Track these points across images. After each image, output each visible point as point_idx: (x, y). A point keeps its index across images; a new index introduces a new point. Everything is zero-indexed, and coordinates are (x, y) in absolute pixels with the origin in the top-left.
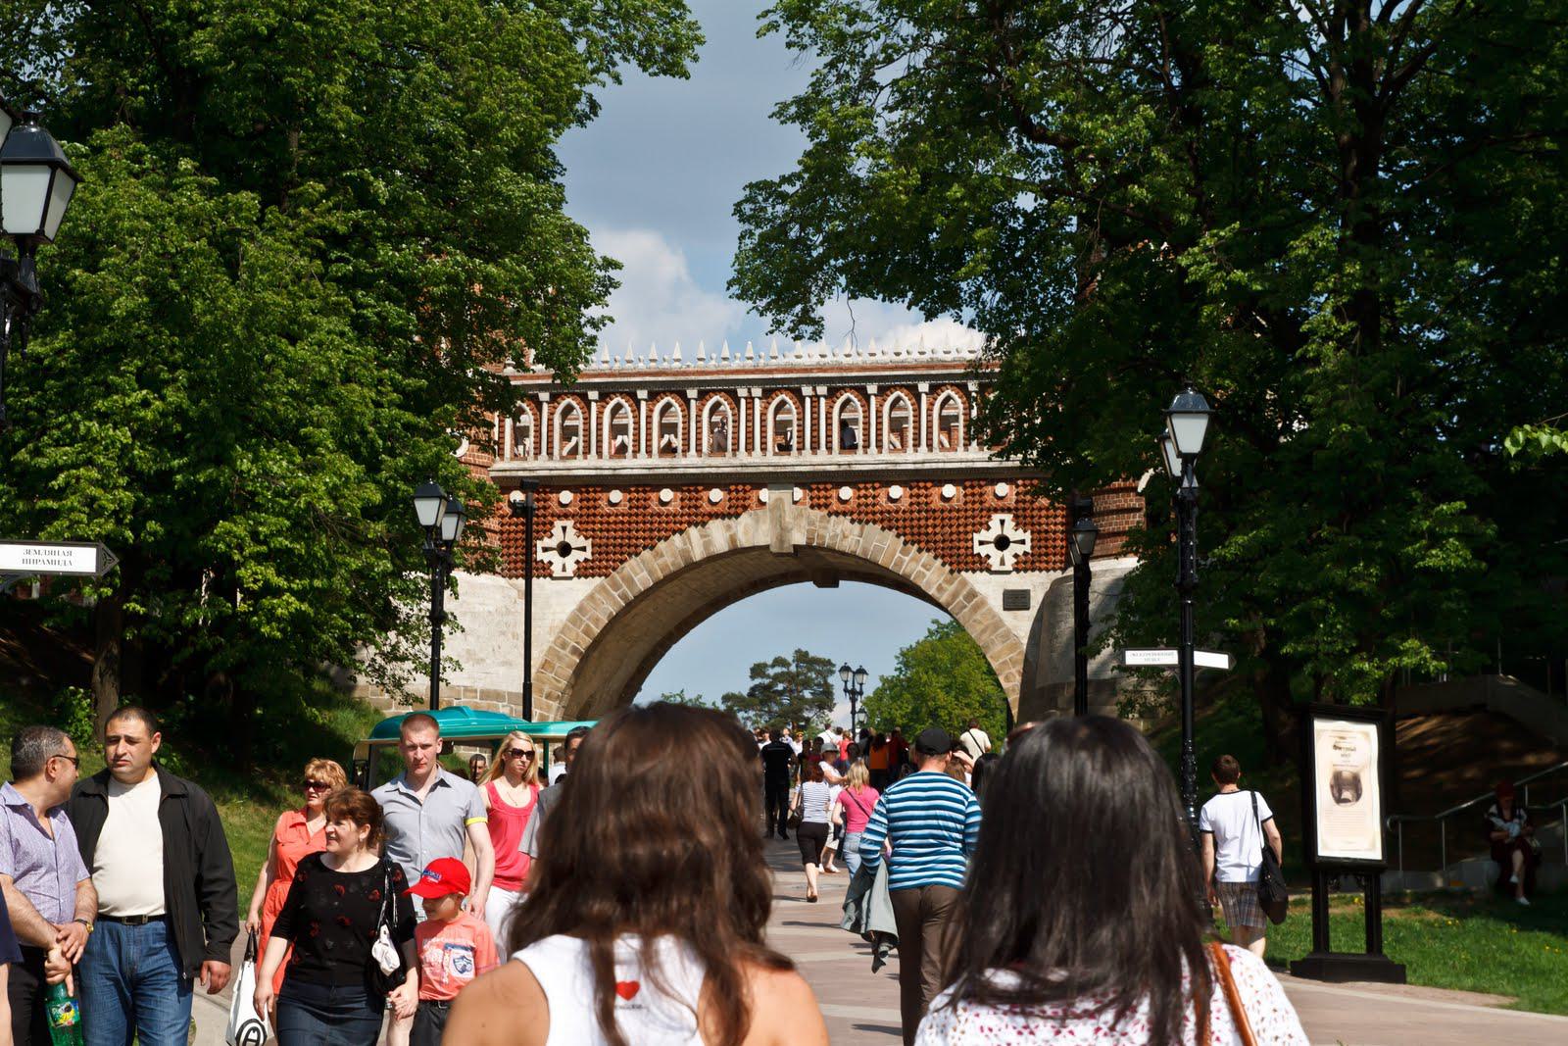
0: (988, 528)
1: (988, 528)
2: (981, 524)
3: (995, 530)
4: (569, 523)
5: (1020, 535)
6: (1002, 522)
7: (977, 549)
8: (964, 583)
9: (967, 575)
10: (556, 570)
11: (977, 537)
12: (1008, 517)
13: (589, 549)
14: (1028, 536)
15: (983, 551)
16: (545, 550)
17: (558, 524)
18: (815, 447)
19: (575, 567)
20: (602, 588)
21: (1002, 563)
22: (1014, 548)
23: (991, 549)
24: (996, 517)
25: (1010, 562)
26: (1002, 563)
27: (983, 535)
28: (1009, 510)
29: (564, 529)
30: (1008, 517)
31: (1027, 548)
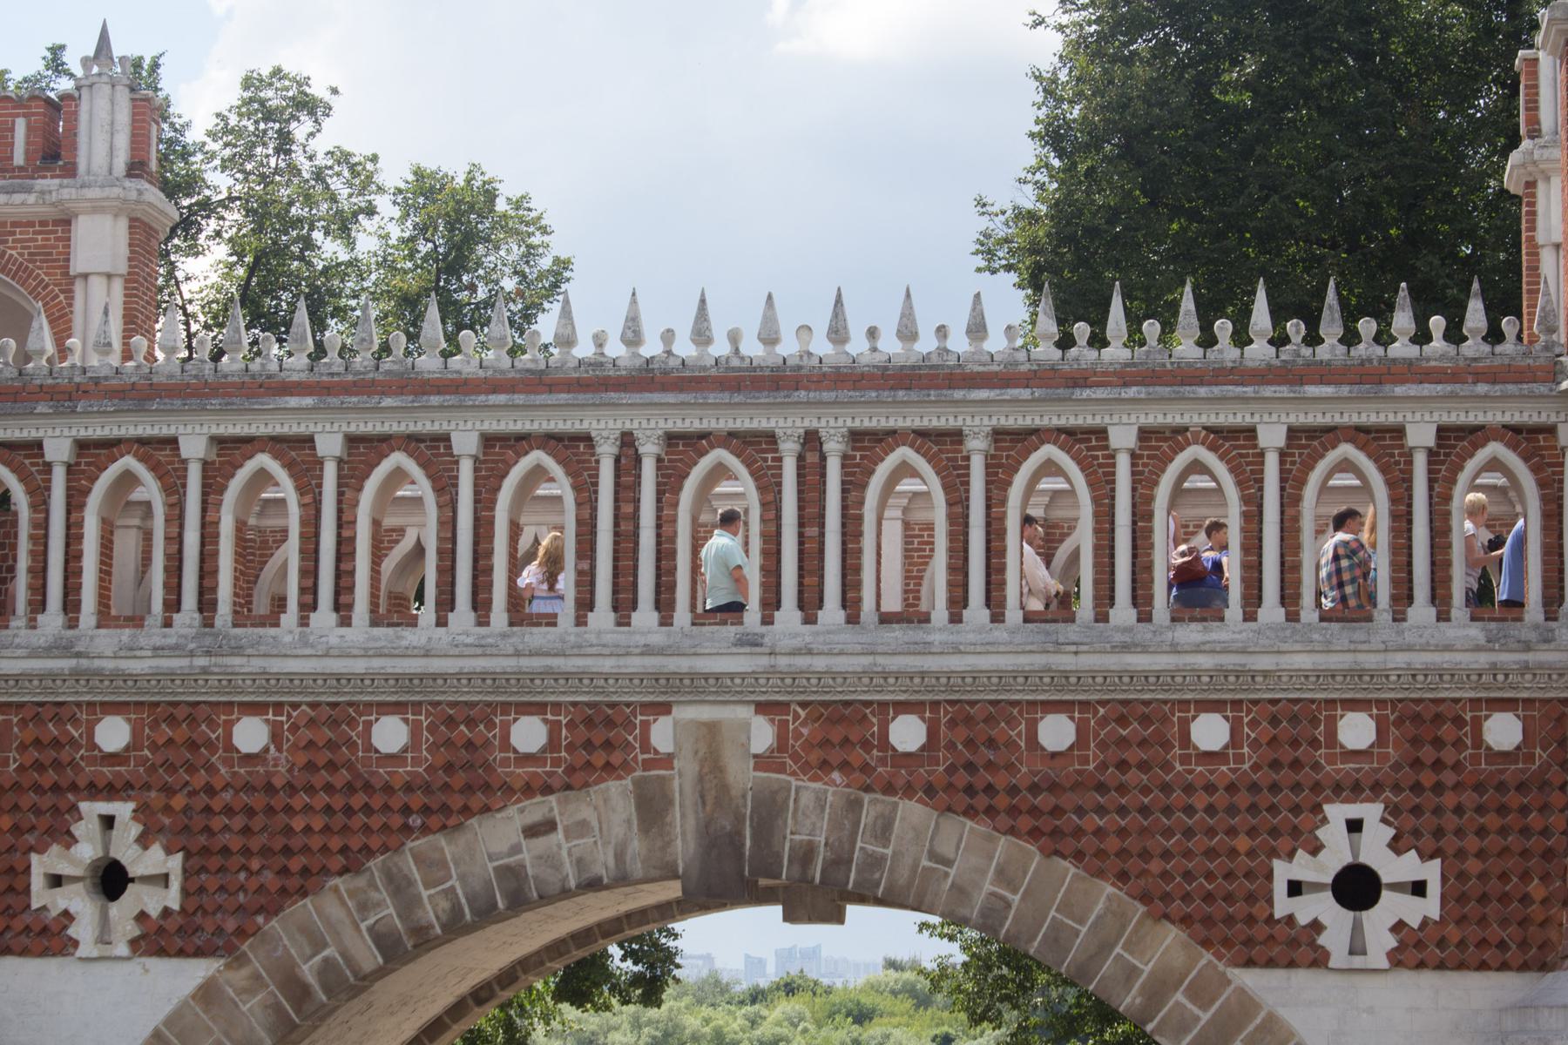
0: (1315, 849)
1: (1315, 849)
2: (1295, 832)
3: (1336, 853)
4: (123, 810)
5: (1408, 866)
6: (1355, 826)
7: (1283, 905)
8: (1246, 1005)
9: (1251, 980)
10: (83, 930)
11: (1283, 872)
12: (1371, 812)
13: (175, 884)
14: (1431, 872)
15: (1306, 909)
16: (56, 881)
17: (92, 809)
18: (810, 603)
19: (133, 930)
20: (207, 993)
21: (1357, 948)
22: (1391, 907)
23: (1321, 907)
24: (1337, 813)
25: (1380, 941)
26: (1357, 948)
27: (1301, 867)
28: (1376, 790)
29: (108, 822)
30: (1371, 812)
31: (1431, 906)
